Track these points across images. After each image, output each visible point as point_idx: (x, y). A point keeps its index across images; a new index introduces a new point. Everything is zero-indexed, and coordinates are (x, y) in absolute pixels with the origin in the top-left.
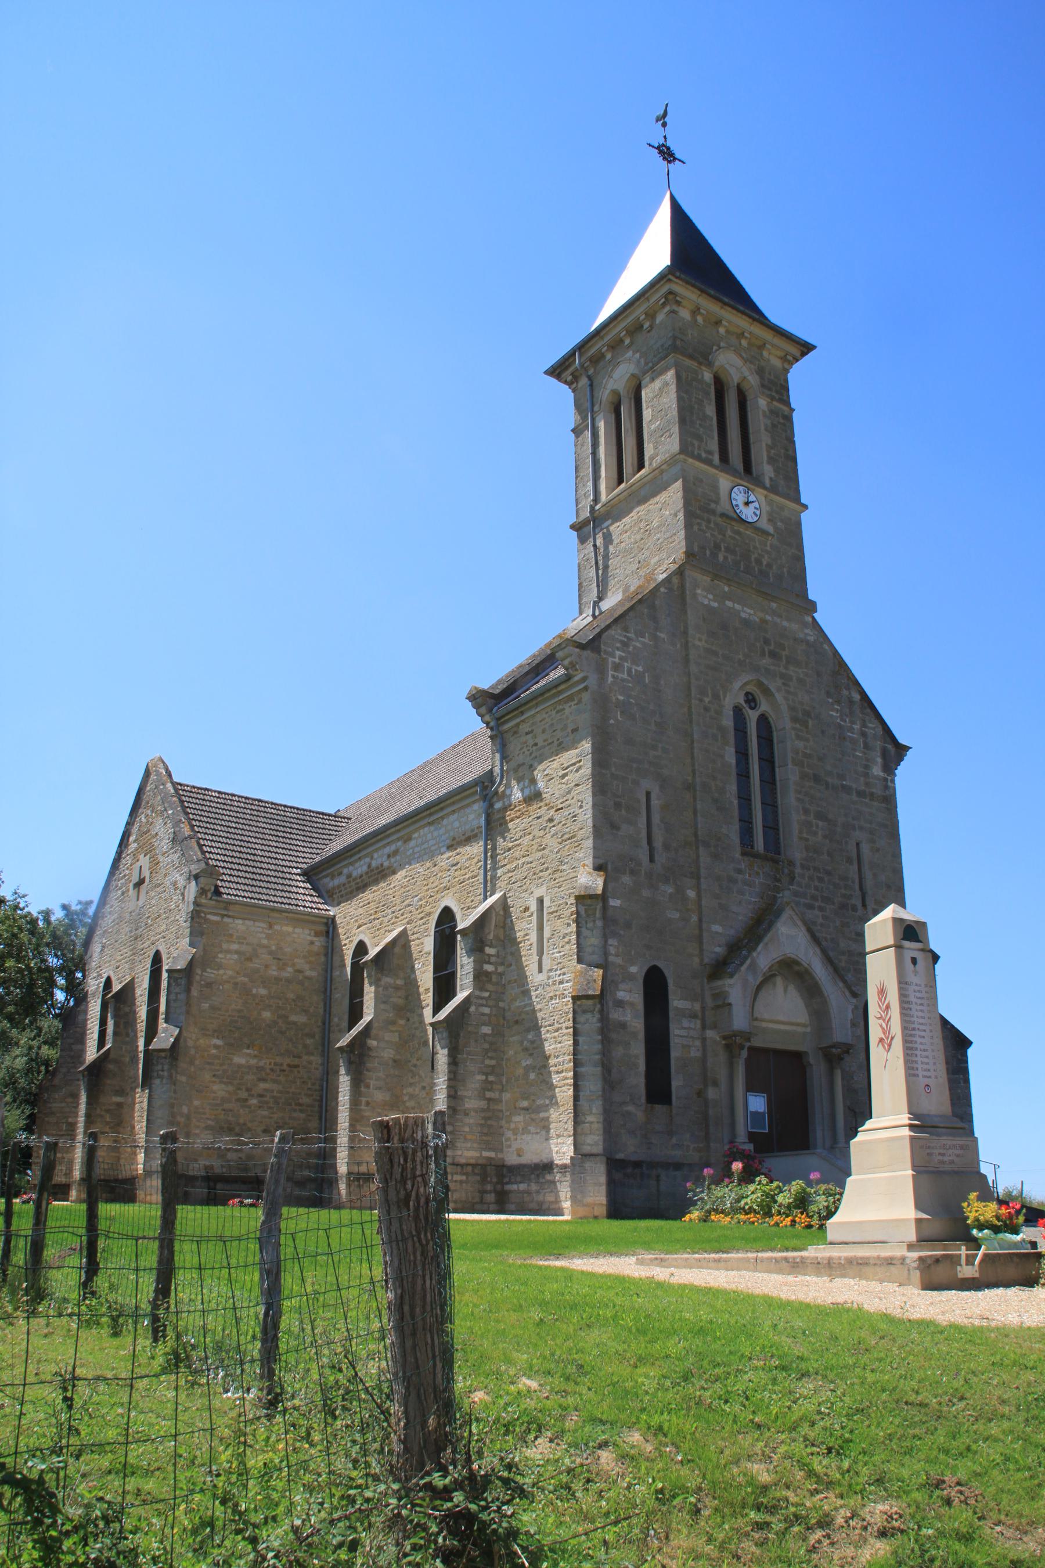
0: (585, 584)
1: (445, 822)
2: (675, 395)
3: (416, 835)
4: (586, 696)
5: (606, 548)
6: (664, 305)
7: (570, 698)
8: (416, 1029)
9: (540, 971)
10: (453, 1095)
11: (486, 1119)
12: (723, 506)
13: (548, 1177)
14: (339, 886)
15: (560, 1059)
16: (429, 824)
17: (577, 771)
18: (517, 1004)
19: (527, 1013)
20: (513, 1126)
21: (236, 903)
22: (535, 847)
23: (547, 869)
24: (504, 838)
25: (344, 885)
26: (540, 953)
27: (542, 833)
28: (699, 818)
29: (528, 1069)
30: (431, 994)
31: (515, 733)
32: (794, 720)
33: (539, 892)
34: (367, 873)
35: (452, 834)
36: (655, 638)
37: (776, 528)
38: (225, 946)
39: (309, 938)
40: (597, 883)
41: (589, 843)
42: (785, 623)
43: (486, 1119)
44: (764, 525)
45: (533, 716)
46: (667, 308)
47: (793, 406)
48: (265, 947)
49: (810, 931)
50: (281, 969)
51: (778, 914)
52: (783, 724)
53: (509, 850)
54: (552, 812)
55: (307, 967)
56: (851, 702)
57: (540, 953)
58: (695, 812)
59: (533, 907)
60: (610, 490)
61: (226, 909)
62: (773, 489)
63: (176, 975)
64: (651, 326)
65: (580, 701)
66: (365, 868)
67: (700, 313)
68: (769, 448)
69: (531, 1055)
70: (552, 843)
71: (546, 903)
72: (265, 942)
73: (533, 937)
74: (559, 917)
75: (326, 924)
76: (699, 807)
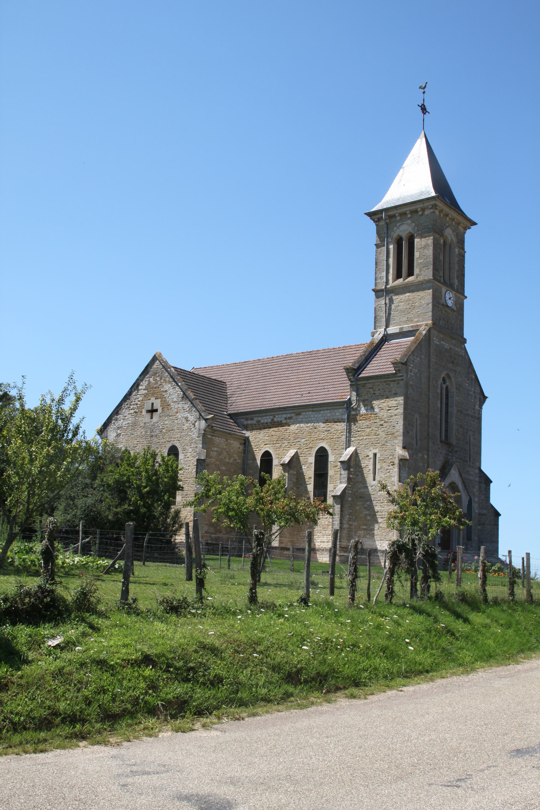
0: (378, 317)
1: (322, 412)
2: (432, 252)
3: (304, 414)
4: (402, 383)
5: (390, 306)
6: (431, 208)
7: (394, 381)
8: (303, 492)
9: (374, 480)
10: (341, 523)
11: (349, 531)
12: (442, 301)
13: (376, 554)
14: (251, 425)
15: (383, 513)
16: (313, 411)
17: (396, 409)
18: (362, 490)
19: (367, 495)
20: (358, 534)
21: (218, 431)
22: (373, 434)
23: (379, 443)
24: (355, 425)
25: (255, 425)
26: (374, 473)
27: (376, 429)
28: (430, 429)
29: (366, 515)
30: (313, 479)
31: (364, 386)
32: (457, 389)
33: (376, 451)
34: (271, 423)
35: (326, 418)
36: (421, 358)
37: (457, 308)
38: (213, 449)
39: (238, 446)
40: (406, 454)
41: (401, 438)
42: (457, 349)
43: (349, 531)
44: (454, 308)
45: (374, 382)
46: (432, 210)
47: (465, 250)
48: (225, 449)
49: (459, 472)
50: (230, 459)
51: (451, 465)
52: (453, 390)
53: (359, 431)
54: (382, 422)
55: (237, 458)
56: (472, 379)
57: (374, 473)
58: (428, 426)
59: (371, 456)
60: (394, 280)
61: (213, 433)
62: (457, 291)
63: (201, 461)
64: (422, 214)
65: (398, 384)
66: (269, 420)
67: (442, 212)
68: (457, 271)
69: (368, 510)
70: (383, 435)
71: (378, 456)
72: (225, 447)
73: (371, 467)
74: (385, 462)
75: (245, 440)
76: (430, 425)
